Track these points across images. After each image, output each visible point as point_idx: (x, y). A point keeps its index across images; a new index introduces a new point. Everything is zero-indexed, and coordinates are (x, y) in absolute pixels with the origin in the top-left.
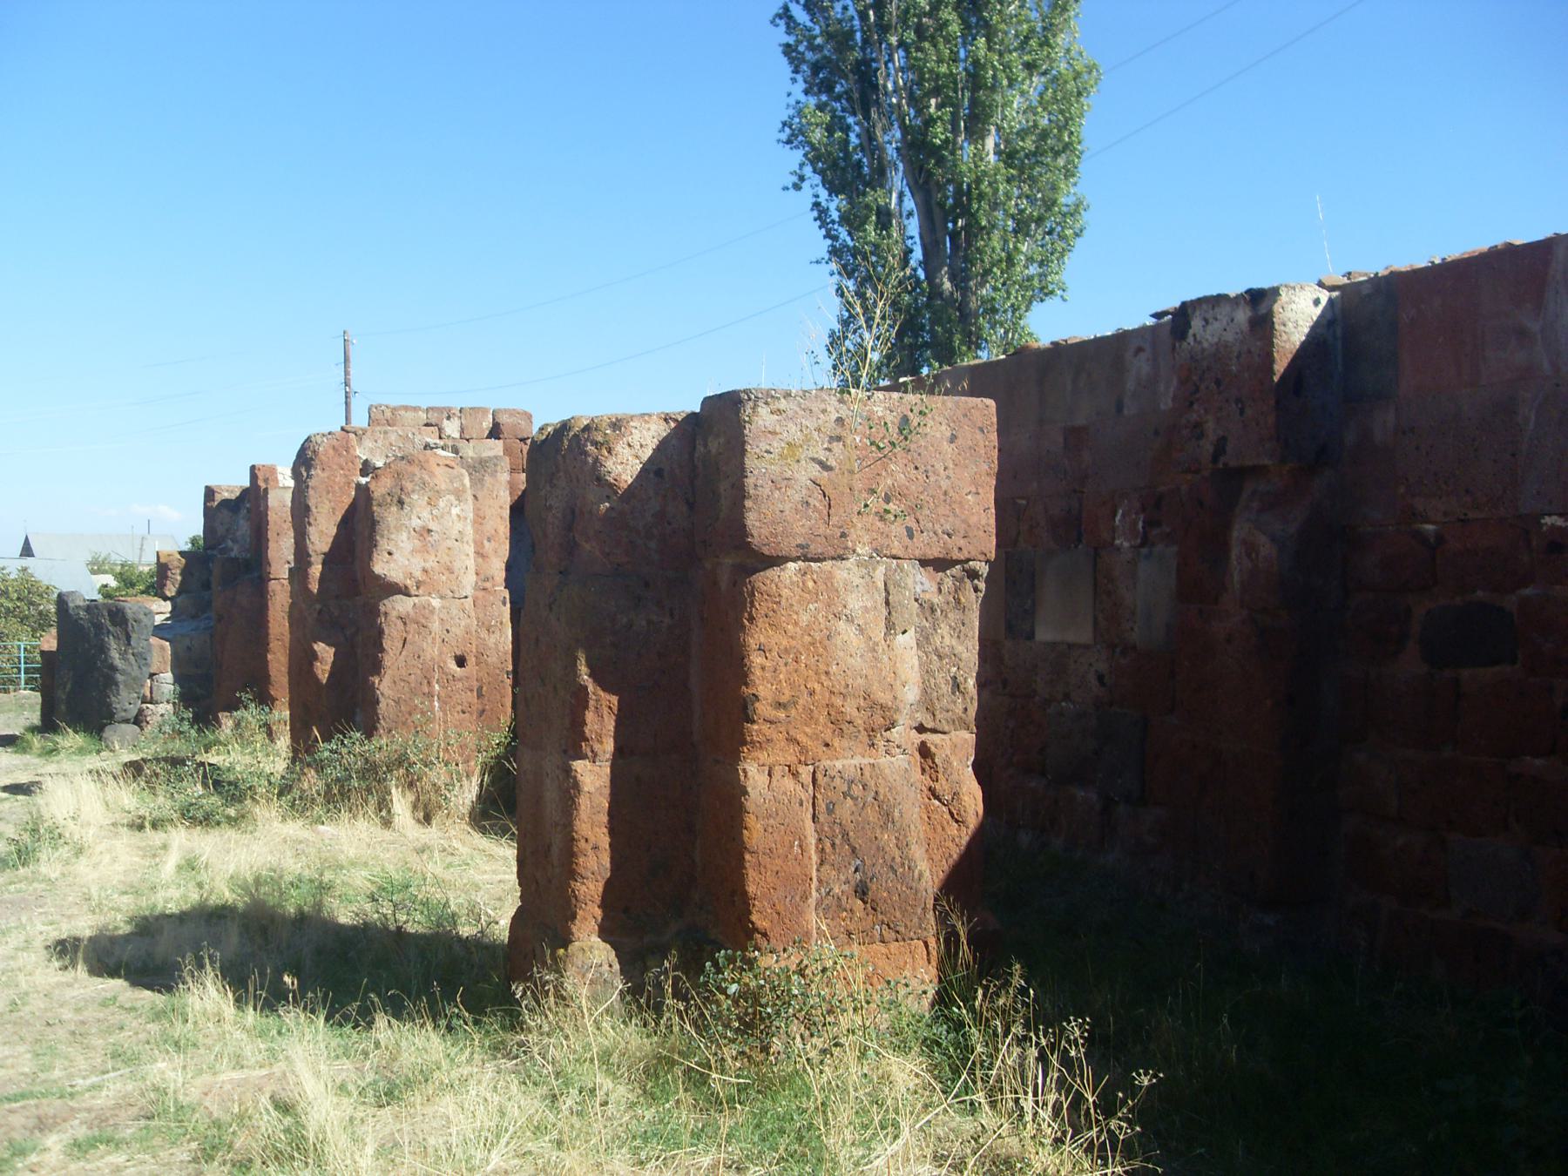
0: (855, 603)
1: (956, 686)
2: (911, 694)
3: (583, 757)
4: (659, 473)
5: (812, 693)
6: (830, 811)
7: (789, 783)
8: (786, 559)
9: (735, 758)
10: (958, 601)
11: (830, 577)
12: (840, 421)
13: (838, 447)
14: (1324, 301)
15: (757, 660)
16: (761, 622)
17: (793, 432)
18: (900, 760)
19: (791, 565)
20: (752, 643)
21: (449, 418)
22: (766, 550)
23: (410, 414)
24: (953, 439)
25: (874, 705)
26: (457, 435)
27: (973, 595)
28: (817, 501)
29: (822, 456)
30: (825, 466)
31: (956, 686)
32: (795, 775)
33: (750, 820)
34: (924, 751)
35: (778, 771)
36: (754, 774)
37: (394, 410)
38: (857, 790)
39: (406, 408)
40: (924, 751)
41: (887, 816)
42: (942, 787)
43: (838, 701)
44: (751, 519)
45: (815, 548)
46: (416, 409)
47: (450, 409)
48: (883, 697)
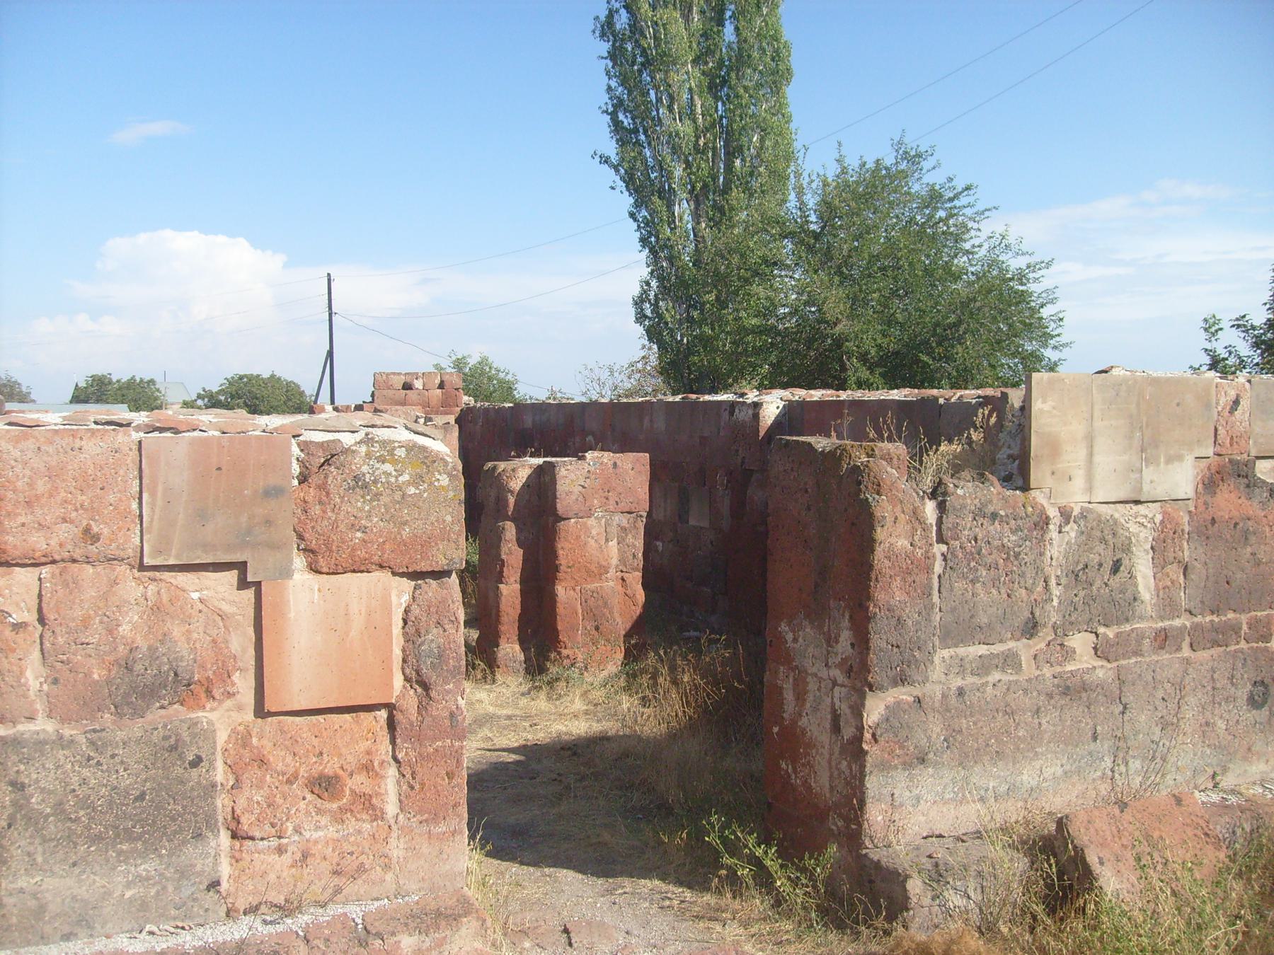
0: (594, 532)
1: (634, 556)
2: (614, 561)
3: (502, 583)
4: (528, 486)
5: (579, 563)
6: (586, 602)
7: (572, 592)
8: (570, 519)
9: (554, 584)
10: (635, 526)
11: (586, 523)
12: (589, 471)
13: (588, 480)
14: (781, 407)
15: (561, 552)
16: (562, 540)
17: (572, 476)
18: (611, 584)
19: (572, 520)
20: (559, 546)
21: (417, 379)
22: (564, 516)
23: (397, 377)
24: (633, 469)
25: (601, 566)
26: (421, 388)
27: (641, 524)
28: (581, 499)
29: (583, 484)
30: (583, 487)
31: (634, 556)
32: (574, 590)
33: (558, 605)
34: (623, 579)
35: (568, 588)
36: (560, 590)
37: (388, 375)
38: (595, 595)
39: (394, 374)
40: (623, 579)
41: (606, 603)
42: (629, 592)
43: (588, 565)
44: (559, 506)
45: (580, 515)
46: (399, 374)
47: (417, 373)
48: (604, 563)
